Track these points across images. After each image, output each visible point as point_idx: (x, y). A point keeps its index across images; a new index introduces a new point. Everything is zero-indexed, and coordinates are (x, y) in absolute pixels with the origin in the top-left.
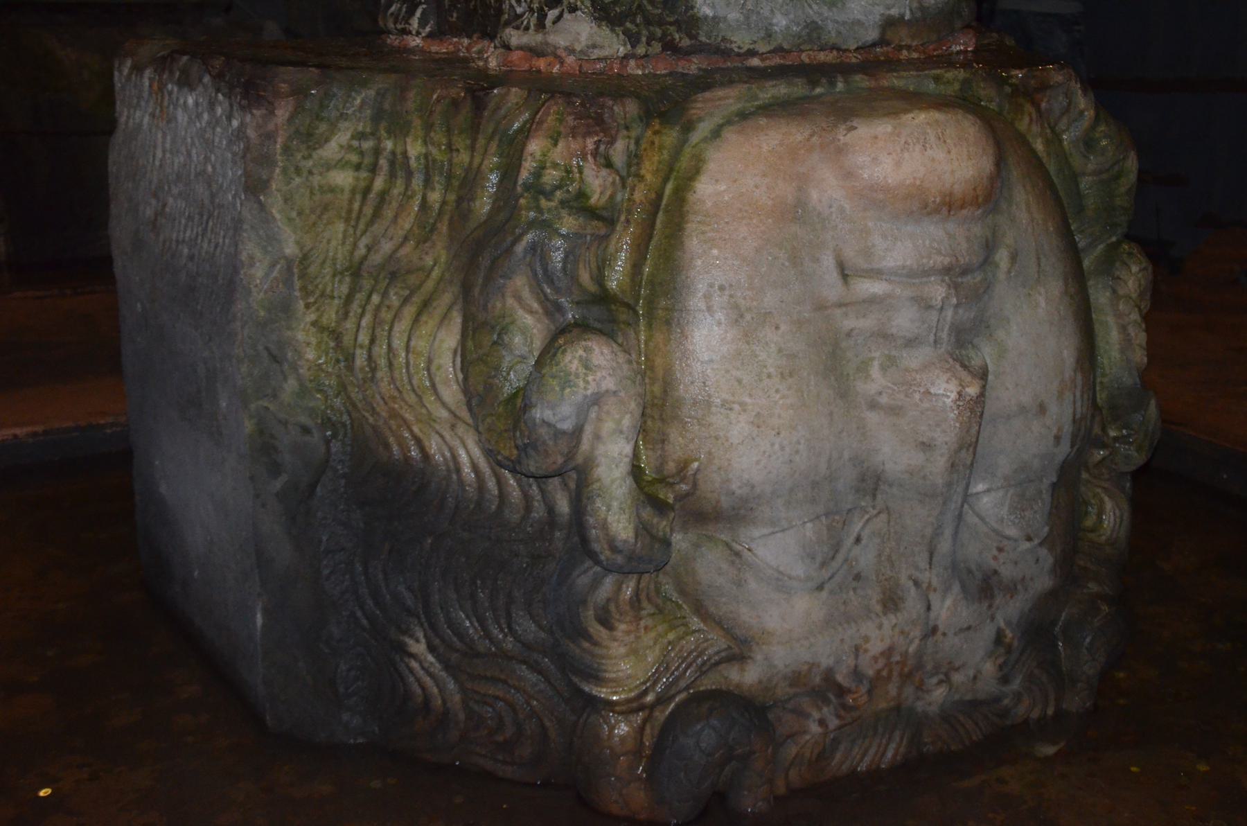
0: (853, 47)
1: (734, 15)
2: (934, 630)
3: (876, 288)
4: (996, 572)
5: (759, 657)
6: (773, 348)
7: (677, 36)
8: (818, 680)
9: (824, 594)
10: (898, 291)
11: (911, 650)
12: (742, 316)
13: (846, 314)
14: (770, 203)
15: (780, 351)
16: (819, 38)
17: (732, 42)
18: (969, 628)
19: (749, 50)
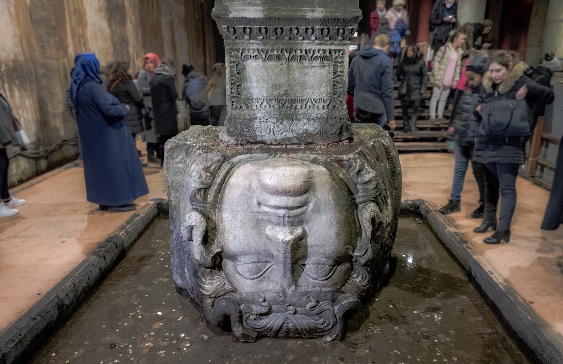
3: (267, 209)
6: (239, 220)
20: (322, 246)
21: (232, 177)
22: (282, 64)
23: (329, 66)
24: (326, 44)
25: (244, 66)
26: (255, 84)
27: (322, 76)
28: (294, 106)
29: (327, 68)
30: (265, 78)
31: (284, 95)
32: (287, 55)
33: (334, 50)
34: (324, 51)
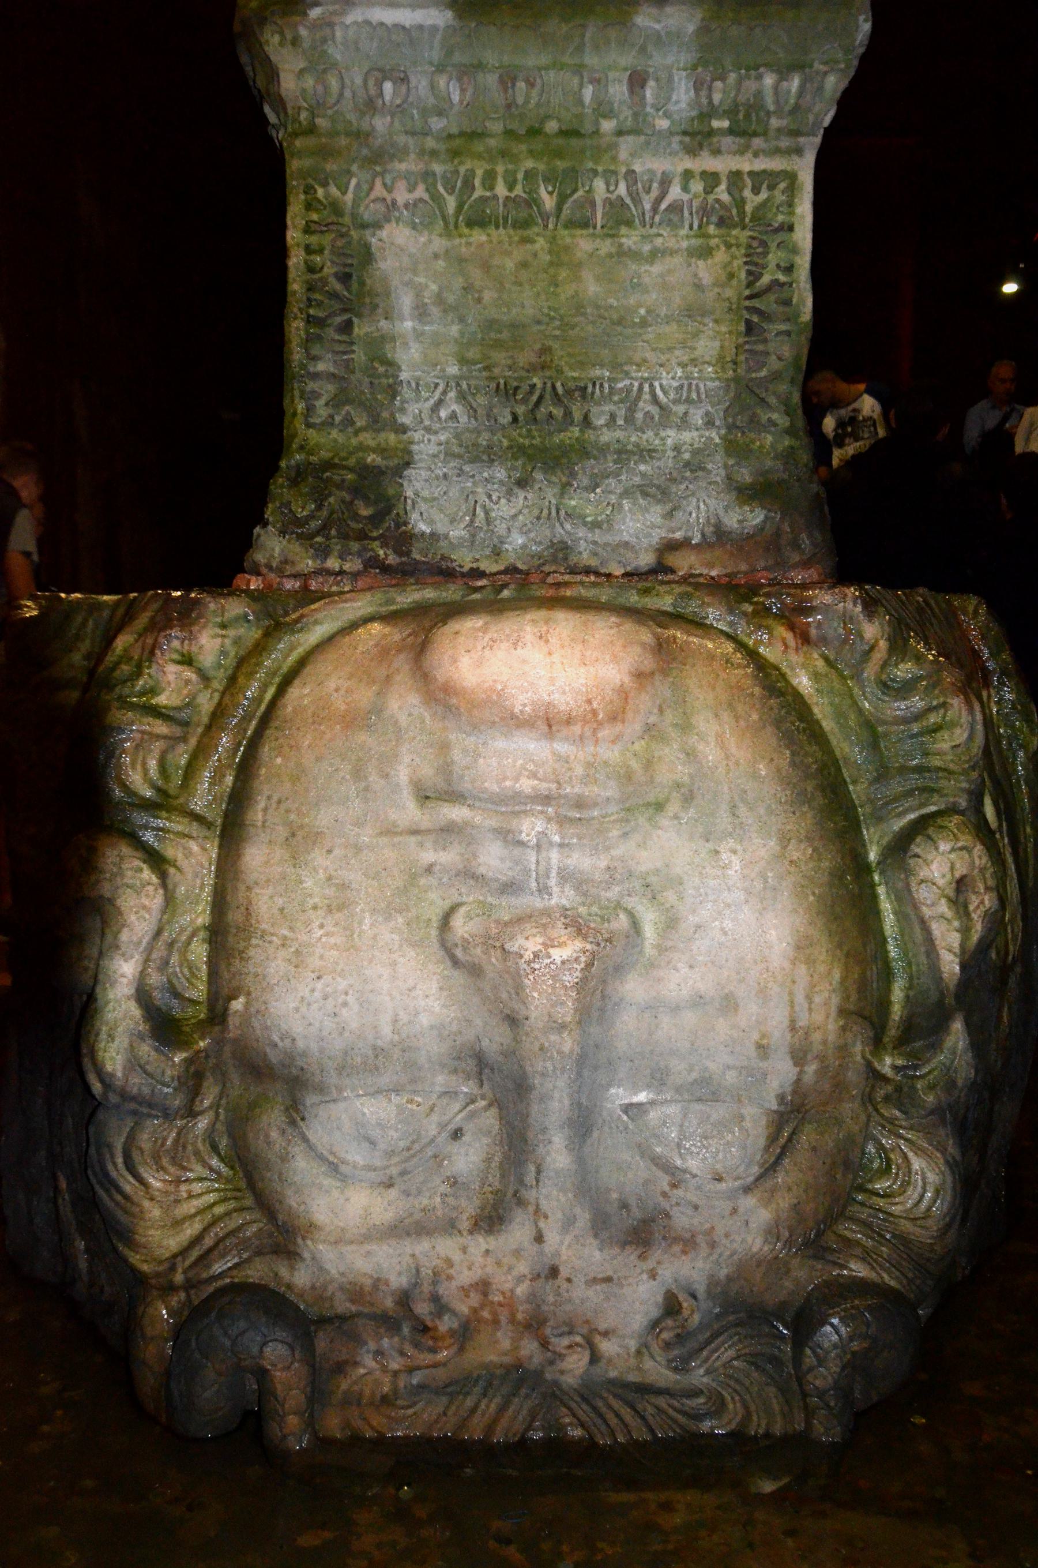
0: (618, 572)
1: (458, 533)
2: (554, 1272)
4: (668, 1216)
5: (306, 1255)
6: (321, 874)
7: (381, 552)
8: (389, 1303)
9: (393, 1193)
10: (478, 819)
11: (519, 1291)
12: (293, 835)
13: (421, 845)
14: (343, 707)
15: (330, 878)
16: (566, 559)
17: (452, 561)
18: (608, 1280)
19: (472, 569)
20: (729, 1004)
21: (297, 682)
22: (526, 240)
23: (728, 246)
24: (717, 152)
25: (367, 247)
26: (408, 324)
27: (698, 287)
28: (577, 416)
29: (721, 256)
30: (451, 299)
31: (532, 369)
32: (549, 202)
33: (751, 173)
34: (711, 179)
